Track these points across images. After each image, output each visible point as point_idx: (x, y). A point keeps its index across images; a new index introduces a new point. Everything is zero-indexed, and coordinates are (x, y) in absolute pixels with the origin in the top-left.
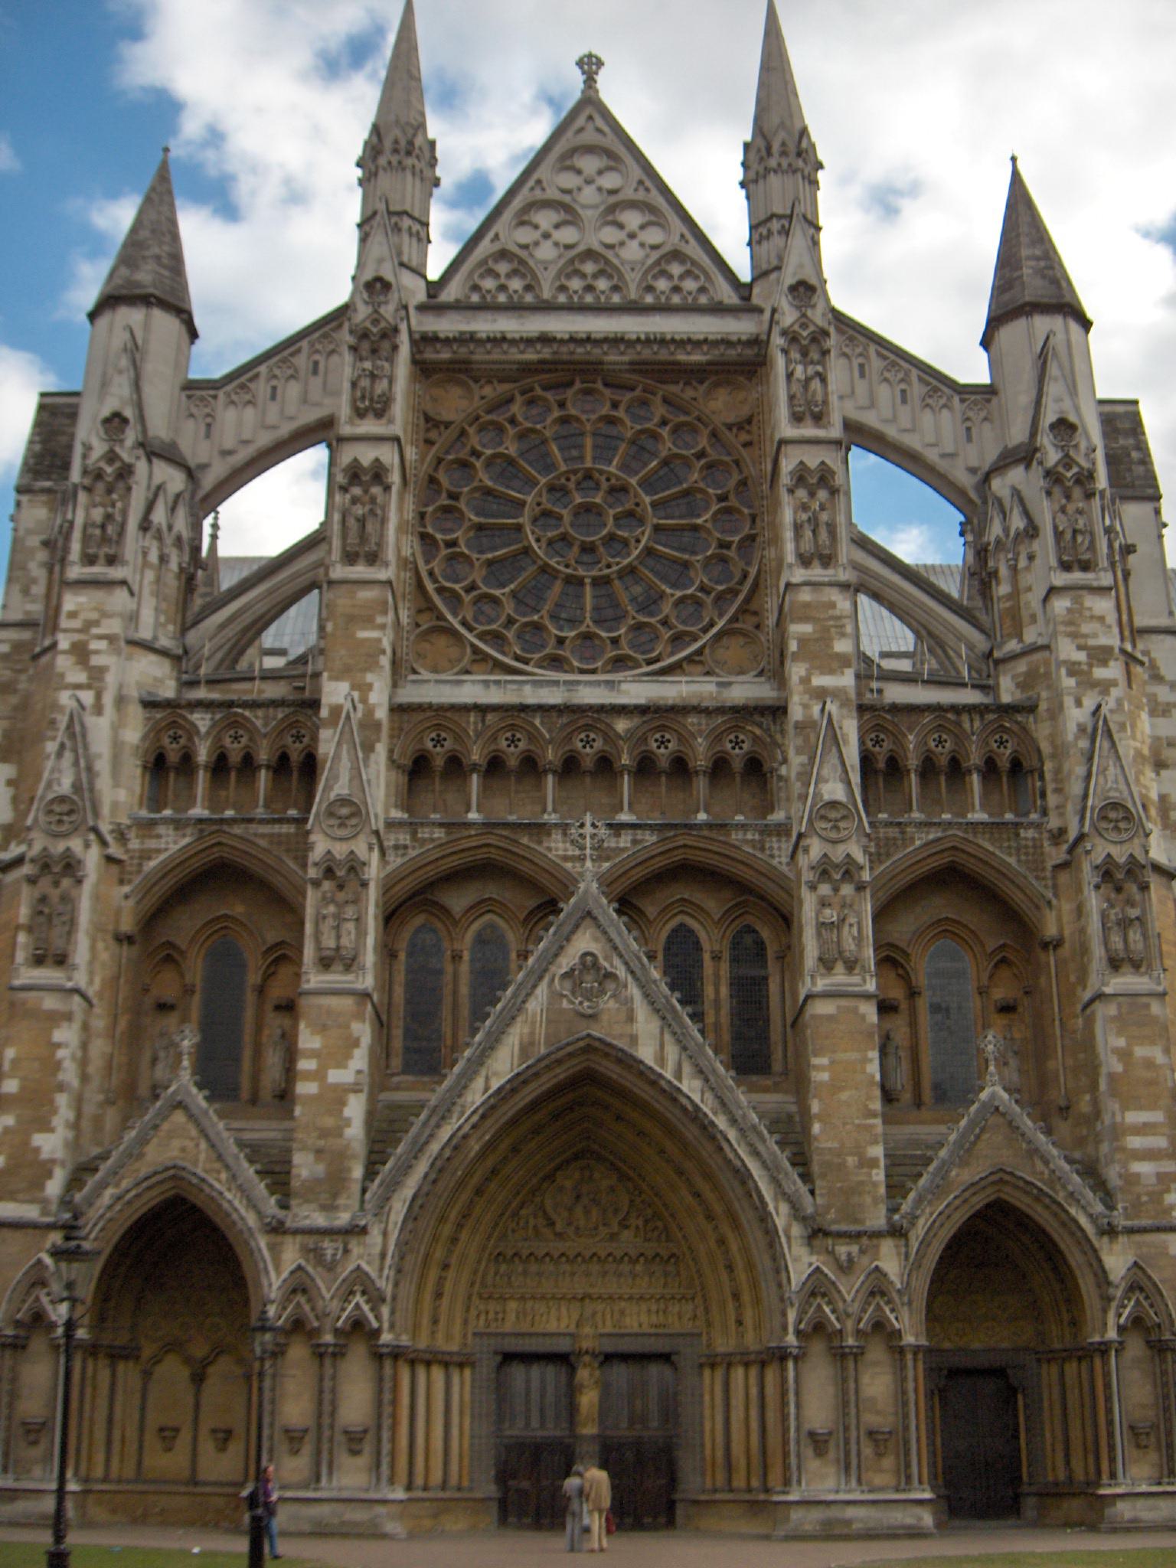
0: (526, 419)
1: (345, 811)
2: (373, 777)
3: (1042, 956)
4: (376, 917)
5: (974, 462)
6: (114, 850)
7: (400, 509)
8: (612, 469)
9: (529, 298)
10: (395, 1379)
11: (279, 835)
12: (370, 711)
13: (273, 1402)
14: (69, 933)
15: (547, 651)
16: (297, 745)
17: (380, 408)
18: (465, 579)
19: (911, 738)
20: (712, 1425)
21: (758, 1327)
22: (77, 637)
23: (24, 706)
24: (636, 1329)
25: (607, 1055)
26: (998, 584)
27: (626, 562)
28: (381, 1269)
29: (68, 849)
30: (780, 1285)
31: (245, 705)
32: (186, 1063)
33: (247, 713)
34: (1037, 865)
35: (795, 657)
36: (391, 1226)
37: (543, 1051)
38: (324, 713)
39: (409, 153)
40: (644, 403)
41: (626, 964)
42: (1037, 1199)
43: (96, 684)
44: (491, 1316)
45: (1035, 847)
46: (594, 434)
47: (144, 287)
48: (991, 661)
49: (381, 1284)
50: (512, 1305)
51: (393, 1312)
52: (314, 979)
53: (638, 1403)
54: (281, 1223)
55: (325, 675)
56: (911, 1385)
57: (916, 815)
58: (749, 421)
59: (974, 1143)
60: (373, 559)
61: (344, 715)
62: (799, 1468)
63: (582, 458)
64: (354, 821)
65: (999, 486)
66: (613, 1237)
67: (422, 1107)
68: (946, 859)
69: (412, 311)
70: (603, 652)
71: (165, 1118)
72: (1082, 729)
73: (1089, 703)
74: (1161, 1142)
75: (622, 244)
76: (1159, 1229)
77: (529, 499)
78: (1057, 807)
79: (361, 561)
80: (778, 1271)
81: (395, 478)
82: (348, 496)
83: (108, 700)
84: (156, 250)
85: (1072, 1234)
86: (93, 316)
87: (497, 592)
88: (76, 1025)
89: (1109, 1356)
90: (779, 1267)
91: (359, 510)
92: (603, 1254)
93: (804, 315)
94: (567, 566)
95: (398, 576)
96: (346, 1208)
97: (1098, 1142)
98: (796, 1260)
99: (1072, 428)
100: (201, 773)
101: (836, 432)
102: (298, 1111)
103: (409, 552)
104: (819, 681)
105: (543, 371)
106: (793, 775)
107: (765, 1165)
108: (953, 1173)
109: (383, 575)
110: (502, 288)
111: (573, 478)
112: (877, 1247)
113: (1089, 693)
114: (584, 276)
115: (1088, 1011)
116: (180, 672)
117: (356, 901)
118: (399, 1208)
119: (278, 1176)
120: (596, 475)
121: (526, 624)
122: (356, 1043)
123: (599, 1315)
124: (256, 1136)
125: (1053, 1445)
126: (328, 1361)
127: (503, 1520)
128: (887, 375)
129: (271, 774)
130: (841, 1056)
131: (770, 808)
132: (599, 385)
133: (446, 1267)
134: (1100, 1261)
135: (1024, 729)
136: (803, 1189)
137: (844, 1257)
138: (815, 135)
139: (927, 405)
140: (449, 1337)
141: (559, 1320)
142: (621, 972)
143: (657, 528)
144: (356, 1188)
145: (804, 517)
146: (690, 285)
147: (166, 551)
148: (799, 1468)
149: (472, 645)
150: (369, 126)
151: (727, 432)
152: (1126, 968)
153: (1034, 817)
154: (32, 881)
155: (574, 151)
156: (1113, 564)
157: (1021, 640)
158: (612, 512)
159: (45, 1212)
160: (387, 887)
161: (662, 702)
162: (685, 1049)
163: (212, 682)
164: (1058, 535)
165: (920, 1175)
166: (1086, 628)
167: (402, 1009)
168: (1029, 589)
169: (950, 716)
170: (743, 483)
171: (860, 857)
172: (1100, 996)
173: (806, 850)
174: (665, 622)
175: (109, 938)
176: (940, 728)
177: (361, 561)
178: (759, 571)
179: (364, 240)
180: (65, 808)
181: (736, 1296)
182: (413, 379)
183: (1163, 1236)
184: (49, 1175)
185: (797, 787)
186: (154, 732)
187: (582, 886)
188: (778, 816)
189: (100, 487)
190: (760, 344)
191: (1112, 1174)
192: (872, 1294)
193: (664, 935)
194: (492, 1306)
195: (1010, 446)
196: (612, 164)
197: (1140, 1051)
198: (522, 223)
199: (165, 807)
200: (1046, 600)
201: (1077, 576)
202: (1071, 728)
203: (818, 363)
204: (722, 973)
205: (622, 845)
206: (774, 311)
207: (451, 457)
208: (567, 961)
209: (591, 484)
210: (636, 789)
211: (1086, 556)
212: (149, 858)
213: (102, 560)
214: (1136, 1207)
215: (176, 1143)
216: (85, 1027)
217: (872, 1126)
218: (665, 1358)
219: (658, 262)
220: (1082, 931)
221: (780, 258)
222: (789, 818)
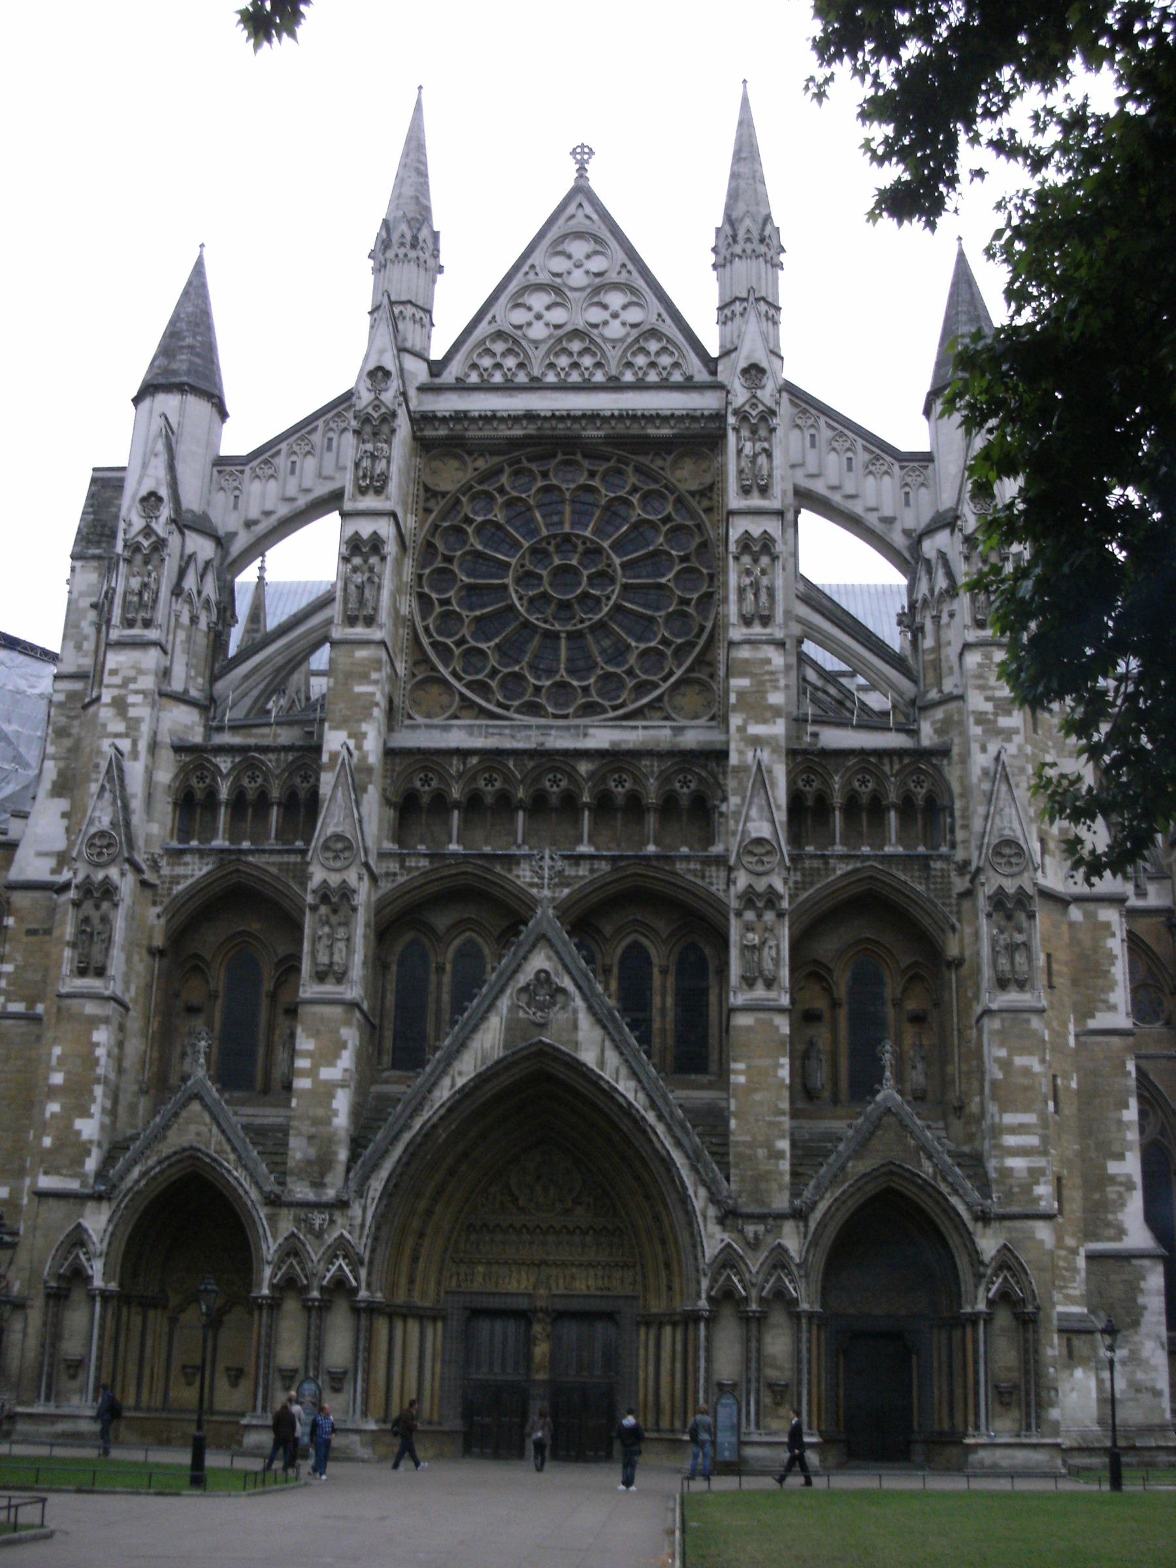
0: (514, 488)
1: (340, 846)
4: (365, 937)
5: (910, 524)
6: (149, 876)
9: (522, 378)
10: (370, 1330)
12: (364, 757)
13: (268, 1346)
14: (107, 949)
15: (526, 698)
16: (305, 785)
17: (378, 485)
19: (837, 778)
20: (644, 1373)
22: (116, 692)
23: (75, 750)
24: (585, 1292)
25: (555, 1059)
26: (924, 637)
28: (360, 1237)
29: (107, 877)
30: (696, 1259)
33: (262, 757)
35: (735, 708)
38: (325, 758)
40: (620, 472)
42: (921, 1188)
43: (132, 733)
44: (462, 1277)
45: (943, 876)
46: (573, 501)
49: (361, 1249)
50: (481, 1269)
51: (369, 1274)
52: (309, 990)
54: (278, 1197)
55: (327, 725)
56: (804, 1347)
57: (839, 849)
58: (711, 488)
59: (869, 1139)
60: (370, 621)
63: (561, 523)
64: (347, 854)
65: (929, 547)
66: (567, 1212)
67: (399, 1100)
69: (412, 393)
71: (184, 1105)
72: (985, 772)
73: (993, 749)
74: (1033, 1140)
75: (606, 323)
77: (513, 561)
79: (361, 622)
80: (695, 1247)
81: (391, 548)
84: (189, 341)
85: (951, 1219)
86: (137, 401)
87: (483, 646)
90: (696, 1243)
91: (358, 578)
92: (558, 1227)
93: (754, 396)
94: (546, 622)
95: (396, 634)
96: (333, 1185)
97: (983, 1138)
98: (711, 1236)
100: (223, 809)
102: (294, 1103)
104: (755, 729)
105: (529, 445)
107: (688, 1157)
109: (377, 634)
110: (498, 366)
112: (780, 1227)
114: (571, 354)
116: (207, 719)
117: (346, 924)
118: (377, 1185)
121: (509, 674)
122: (344, 1046)
124: (266, 1121)
126: (314, 1313)
128: (835, 444)
131: (710, 841)
132: (579, 457)
133: (422, 1235)
134: (973, 1243)
135: (938, 769)
136: (720, 1176)
137: (751, 1235)
138: (777, 221)
139: (871, 473)
140: (423, 1294)
141: (519, 1282)
143: (625, 587)
144: (340, 1169)
145: (747, 581)
146: (665, 360)
149: (461, 694)
151: (690, 498)
152: (1013, 987)
153: (944, 850)
154: (77, 904)
155: (565, 237)
157: (940, 691)
158: (585, 573)
159: (83, 1184)
160: (380, 908)
161: (624, 746)
162: (621, 1054)
163: (235, 728)
167: (392, 1014)
168: (949, 644)
169: (872, 760)
170: (704, 545)
172: (988, 1012)
173: (735, 883)
174: (630, 672)
175: (144, 952)
176: (864, 770)
177: (361, 622)
180: (105, 842)
183: (1031, 1223)
184: (88, 1153)
186: (184, 772)
187: (539, 911)
188: (717, 849)
189: (139, 559)
190: (718, 417)
192: (775, 1267)
193: (619, 951)
195: (942, 509)
196: (598, 248)
197: (1019, 1061)
198: (517, 305)
199: (192, 839)
200: (961, 655)
202: (976, 773)
203: (766, 440)
205: (581, 873)
207: (446, 524)
208: (525, 977)
209: (568, 547)
210: (595, 822)
212: (178, 883)
213: (139, 623)
215: (193, 1128)
216: (121, 1028)
217: (780, 1123)
218: (609, 1316)
219: (637, 340)
220: (978, 954)
222: (727, 850)
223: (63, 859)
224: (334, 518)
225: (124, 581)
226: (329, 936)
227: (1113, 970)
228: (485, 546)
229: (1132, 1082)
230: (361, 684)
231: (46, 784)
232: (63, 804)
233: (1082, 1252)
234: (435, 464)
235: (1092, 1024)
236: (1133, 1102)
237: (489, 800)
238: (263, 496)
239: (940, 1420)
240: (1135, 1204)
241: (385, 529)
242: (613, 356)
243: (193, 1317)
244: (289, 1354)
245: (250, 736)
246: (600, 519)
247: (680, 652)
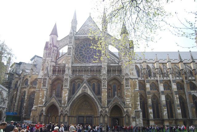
6: (50, 77)
9: (84, 33)
20: (94, 122)
31: (60, 66)
37: (81, 93)
48: (119, 62)
60: (70, 55)
74: (129, 100)
81: (72, 48)
90: (99, 110)
109: (71, 56)
118: (70, 105)
133: (74, 109)
154: (43, 80)
160: (71, 80)
186: (53, 68)
208: (83, 86)
218: (91, 117)
232: (43, 71)
235: (135, 90)
240: (139, 106)
241: (72, 47)
243: (54, 118)
244: (62, 121)
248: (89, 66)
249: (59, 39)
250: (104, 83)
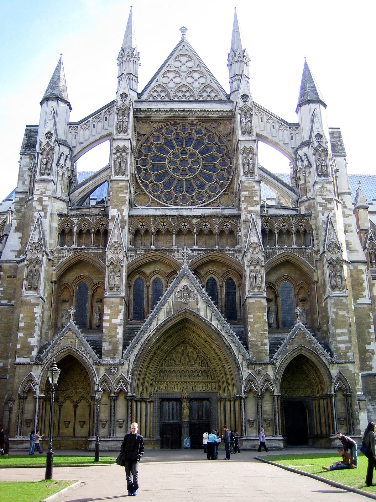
0: (166, 133)
1: (116, 245)
2: (124, 236)
3: (313, 286)
6: (50, 257)
7: (131, 160)
8: (190, 148)
9: (167, 99)
11: (98, 252)
12: (123, 218)
13: (97, 413)
18: (149, 179)
20: (221, 418)
21: (233, 391)
22: (39, 196)
23: (24, 216)
27: (195, 174)
28: (128, 375)
30: (240, 379)
32: (72, 317)
34: (311, 260)
36: (130, 363)
38: (110, 218)
39: (132, 56)
41: (196, 289)
42: (312, 354)
45: (310, 255)
47: (56, 95)
50: (165, 385)
51: (131, 387)
52: (108, 293)
53: (200, 412)
54: (100, 363)
55: (110, 207)
56: (276, 407)
59: (294, 338)
60: (124, 174)
61: (116, 218)
62: (245, 429)
63: (182, 145)
65: (301, 153)
66: (192, 366)
68: (286, 258)
70: (189, 200)
72: (324, 222)
73: (326, 214)
74: (346, 338)
75: (193, 83)
76: (346, 363)
78: (317, 244)
80: (239, 375)
81: (129, 151)
82: (116, 156)
83: (48, 214)
86: (41, 103)
87: (159, 183)
88: (40, 307)
89: (332, 398)
90: (240, 374)
91: (119, 160)
93: (245, 104)
94: (178, 176)
95: (130, 178)
97: (329, 338)
99: (321, 136)
100: (75, 235)
101: (254, 137)
103: (134, 171)
104: (250, 208)
106: (243, 235)
107: (235, 345)
108: (288, 347)
109: (127, 178)
110: (159, 95)
111: (179, 150)
113: (326, 212)
114: (182, 92)
115: (326, 301)
117: (119, 271)
118: (132, 357)
119: (98, 349)
120: (186, 150)
122: (121, 312)
123: (189, 388)
124: (91, 338)
125: (317, 424)
126: (113, 401)
127: (162, 447)
128: (269, 121)
129: (95, 235)
130: (256, 314)
132: (187, 124)
133: (146, 374)
134: (329, 371)
135: (308, 222)
136: (246, 352)
137: (258, 371)
139: (280, 129)
140: (146, 395)
142: (195, 291)
144: (121, 352)
145: (246, 162)
146: (213, 95)
147: (64, 172)
148: (245, 430)
149: (151, 198)
150: (121, 48)
153: (310, 246)
154: (27, 266)
155: (179, 55)
156: (332, 175)
157: (307, 197)
160: (128, 267)
164: (317, 167)
165: (279, 348)
166: (325, 193)
168: (309, 182)
171: (262, 258)
172: (329, 297)
173: (247, 256)
177: (120, 174)
178: (232, 177)
179: (119, 82)
181: (227, 382)
182: (134, 122)
184: (34, 350)
185: (244, 238)
186: (61, 224)
187: (184, 267)
189: (45, 153)
190: (231, 111)
191: (333, 347)
192: (265, 381)
193: (206, 280)
194: (159, 385)
197: (340, 313)
198: (165, 77)
201: (322, 178)
202: (320, 222)
204: (223, 291)
205: (194, 255)
206: (237, 103)
208: (179, 288)
209: (185, 152)
211: (325, 173)
212: (61, 259)
213: (46, 174)
214: (339, 356)
215: (69, 340)
216: (43, 307)
219: (203, 88)
220: (324, 279)
221: (239, 88)
223: (20, 252)
224: (107, 144)
225: (41, 160)
226: (115, 276)
227: (364, 284)
228: (158, 151)
229: (372, 320)
230: (122, 194)
231: (13, 228)
232: (19, 234)
233: (360, 374)
234: (140, 125)
235: (359, 302)
236: (372, 326)
237: (163, 232)
238: (84, 134)
239: (317, 431)
241: (128, 144)
242: (196, 93)
243: (68, 405)
244: (104, 415)
245: (82, 212)
246: (195, 144)
247: (222, 186)
248: (195, 217)
249: (75, 117)
250: (255, 278)
